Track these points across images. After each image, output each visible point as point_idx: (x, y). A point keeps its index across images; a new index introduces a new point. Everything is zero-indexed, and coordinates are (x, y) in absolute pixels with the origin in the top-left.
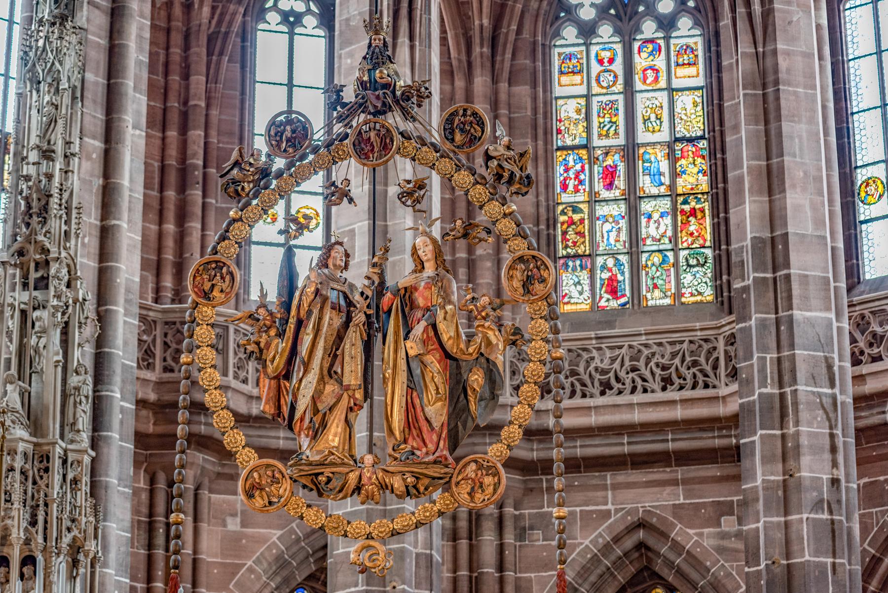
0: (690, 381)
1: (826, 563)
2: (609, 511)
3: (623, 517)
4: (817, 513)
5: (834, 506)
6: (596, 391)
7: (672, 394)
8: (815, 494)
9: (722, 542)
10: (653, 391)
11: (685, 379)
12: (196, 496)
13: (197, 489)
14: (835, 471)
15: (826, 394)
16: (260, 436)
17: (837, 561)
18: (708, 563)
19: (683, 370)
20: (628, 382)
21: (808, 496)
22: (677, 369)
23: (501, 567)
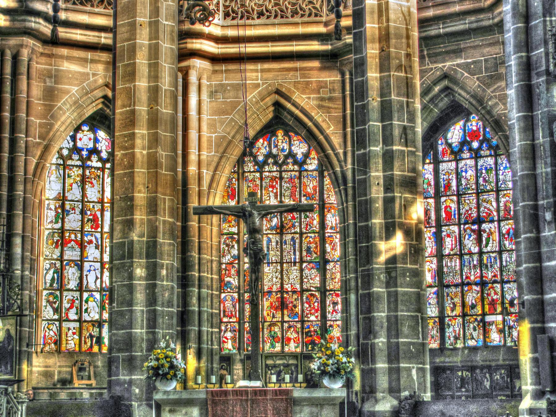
0: (307, 13)
1: (403, 101)
2: (259, 84)
3: (267, 87)
4: (398, 72)
5: (408, 69)
6: (255, 16)
7: (297, 19)
8: (397, 61)
9: (321, 103)
10: (287, 17)
11: (304, 12)
12: (29, 65)
13: (30, 60)
14: (409, 50)
15: (404, 6)
16: (66, 32)
17: (410, 100)
18: (313, 114)
19: (304, 6)
20: (273, 12)
21: (394, 62)
22: (300, 5)
23: (199, 112)
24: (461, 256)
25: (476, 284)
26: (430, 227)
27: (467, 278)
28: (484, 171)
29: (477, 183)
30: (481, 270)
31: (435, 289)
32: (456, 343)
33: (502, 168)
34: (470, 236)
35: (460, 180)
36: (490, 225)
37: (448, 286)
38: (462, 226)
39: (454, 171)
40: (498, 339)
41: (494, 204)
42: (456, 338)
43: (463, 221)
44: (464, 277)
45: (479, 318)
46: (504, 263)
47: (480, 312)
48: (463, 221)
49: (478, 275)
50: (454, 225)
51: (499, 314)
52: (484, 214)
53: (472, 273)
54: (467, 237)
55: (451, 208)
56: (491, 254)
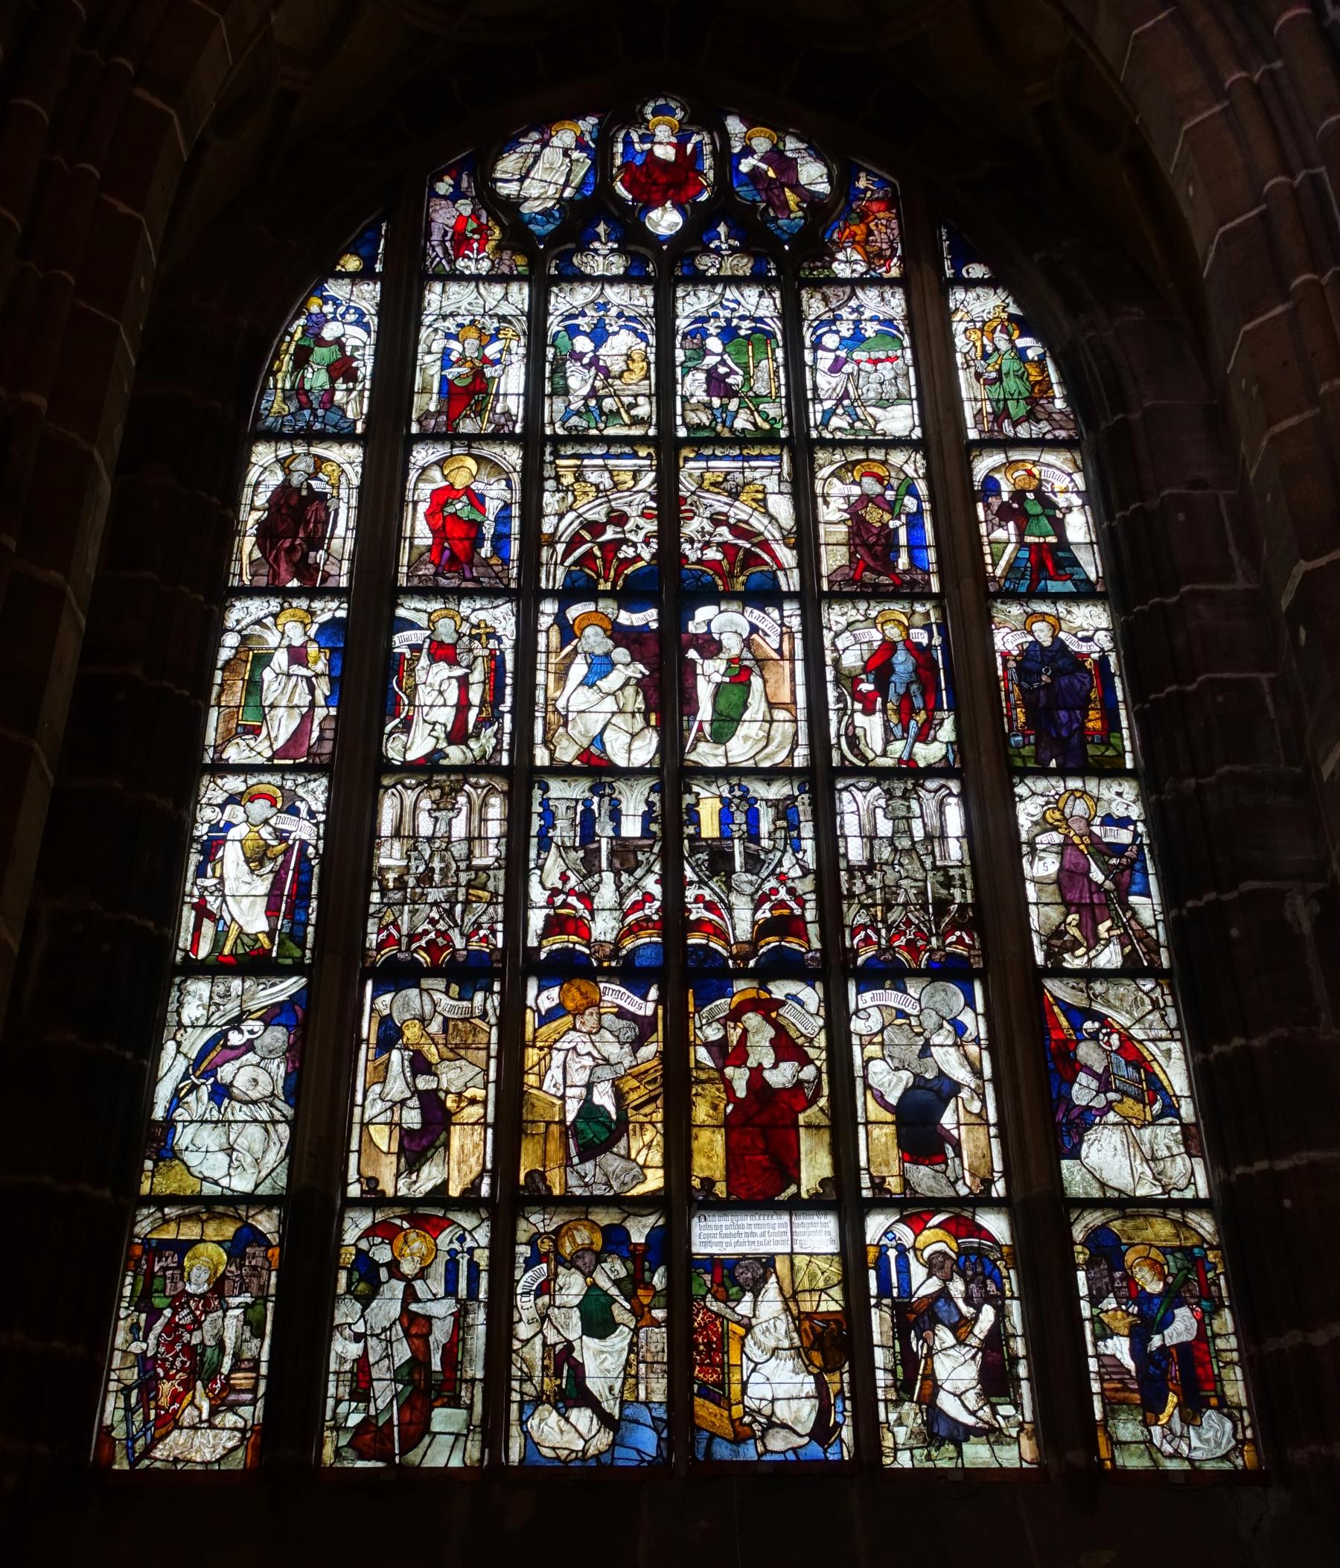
24: (521, 780)
25: (633, 976)
26: (313, 593)
27: (555, 925)
28: (714, 344)
29: (665, 391)
30: (673, 883)
31: (290, 986)
32: (418, 1430)
33: (830, 341)
34: (601, 666)
35: (559, 367)
36: (754, 615)
37: (399, 975)
38: (549, 607)
39: (522, 325)
40: (803, 1414)
41: (782, 507)
42: (425, 1388)
43: (554, 576)
44: (536, 920)
45: (638, 1232)
46: (855, 851)
47: (655, 1180)
48: (554, 576)
49: (651, 909)
50: (492, 593)
51: (815, 1204)
52: (712, 554)
53: (606, 895)
54: (579, 670)
55: (477, 501)
56: (759, 790)
